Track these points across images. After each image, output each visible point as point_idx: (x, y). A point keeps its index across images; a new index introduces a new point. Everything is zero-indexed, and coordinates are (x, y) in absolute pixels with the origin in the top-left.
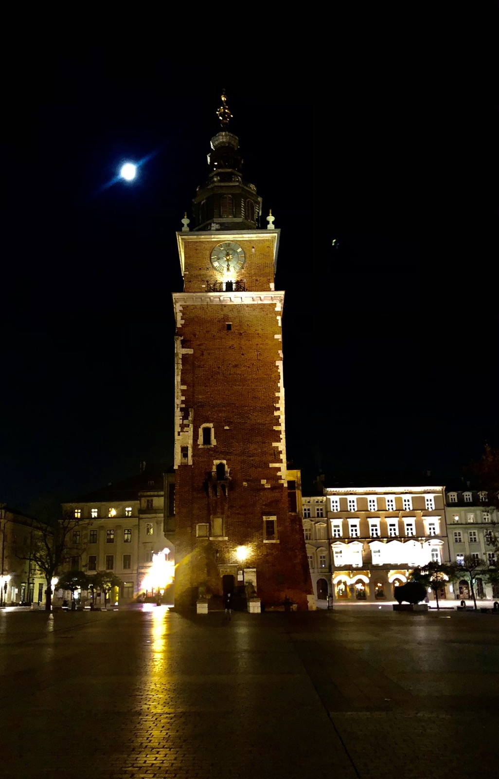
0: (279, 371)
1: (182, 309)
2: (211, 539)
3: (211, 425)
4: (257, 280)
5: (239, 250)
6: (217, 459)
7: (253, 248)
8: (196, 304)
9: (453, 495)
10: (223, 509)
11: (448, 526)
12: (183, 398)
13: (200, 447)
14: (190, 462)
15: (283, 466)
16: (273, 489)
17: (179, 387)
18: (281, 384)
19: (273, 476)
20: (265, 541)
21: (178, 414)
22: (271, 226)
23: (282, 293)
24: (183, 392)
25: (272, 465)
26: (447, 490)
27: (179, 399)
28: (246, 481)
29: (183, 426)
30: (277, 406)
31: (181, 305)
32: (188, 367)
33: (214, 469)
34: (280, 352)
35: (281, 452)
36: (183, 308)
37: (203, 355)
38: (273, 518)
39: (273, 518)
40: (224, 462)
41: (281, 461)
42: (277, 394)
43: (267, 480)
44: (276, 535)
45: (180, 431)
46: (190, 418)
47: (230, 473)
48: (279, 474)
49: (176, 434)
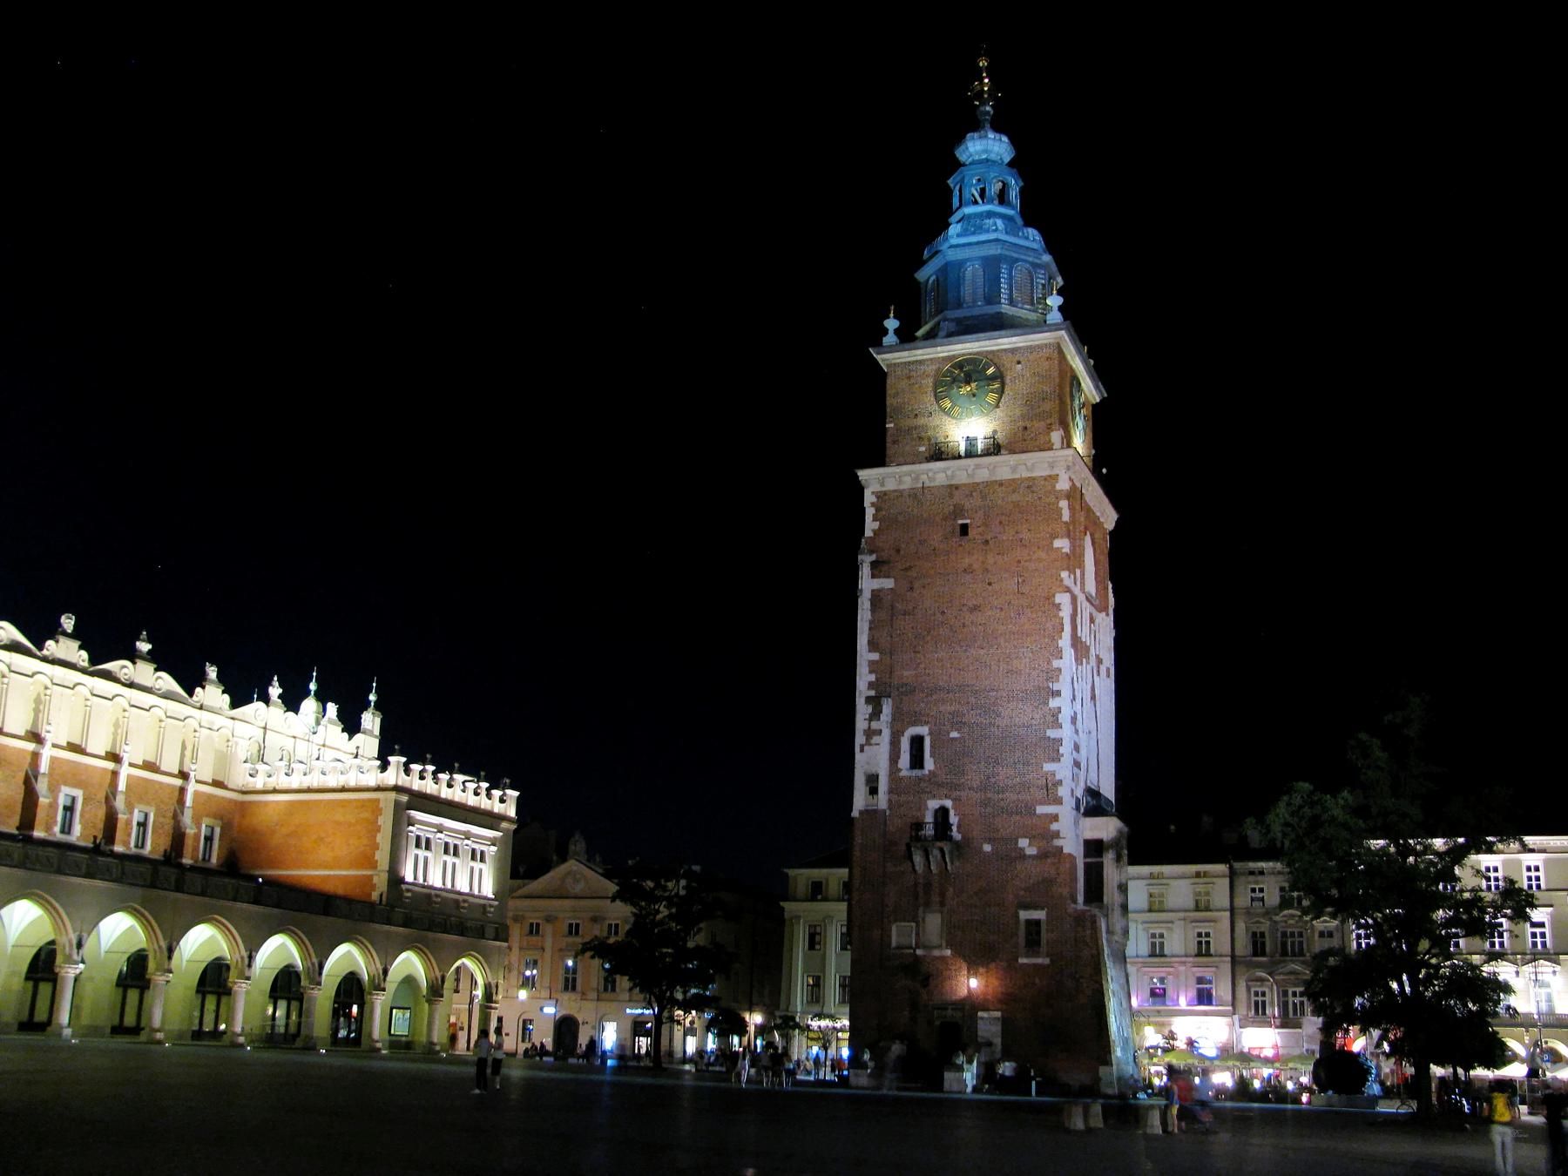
0: (1061, 614)
1: (874, 499)
2: (919, 952)
3: (923, 730)
5: (991, 371)
6: (934, 797)
10: (942, 895)
12: (872, 678)
13: (904, 773)
14: (882, 800)
16: (1043, 856)
17: (865, 656)
19: (1045, 834)
21: (862, 710)
25: (1040, 810)
27: (864, 679)
28: (990, 840)
29: (870, 733)
32: (883, 615)
33: (929, 818)
35: (1060, 782)
38: (1040, 915)
39: (1040, 915)
40: (948, 803)
42: (1056, 663)
43: (1032, 838)
44: (1044, 948)
47: (959, 827)
48: (1054, 827)
49: (857, 749)
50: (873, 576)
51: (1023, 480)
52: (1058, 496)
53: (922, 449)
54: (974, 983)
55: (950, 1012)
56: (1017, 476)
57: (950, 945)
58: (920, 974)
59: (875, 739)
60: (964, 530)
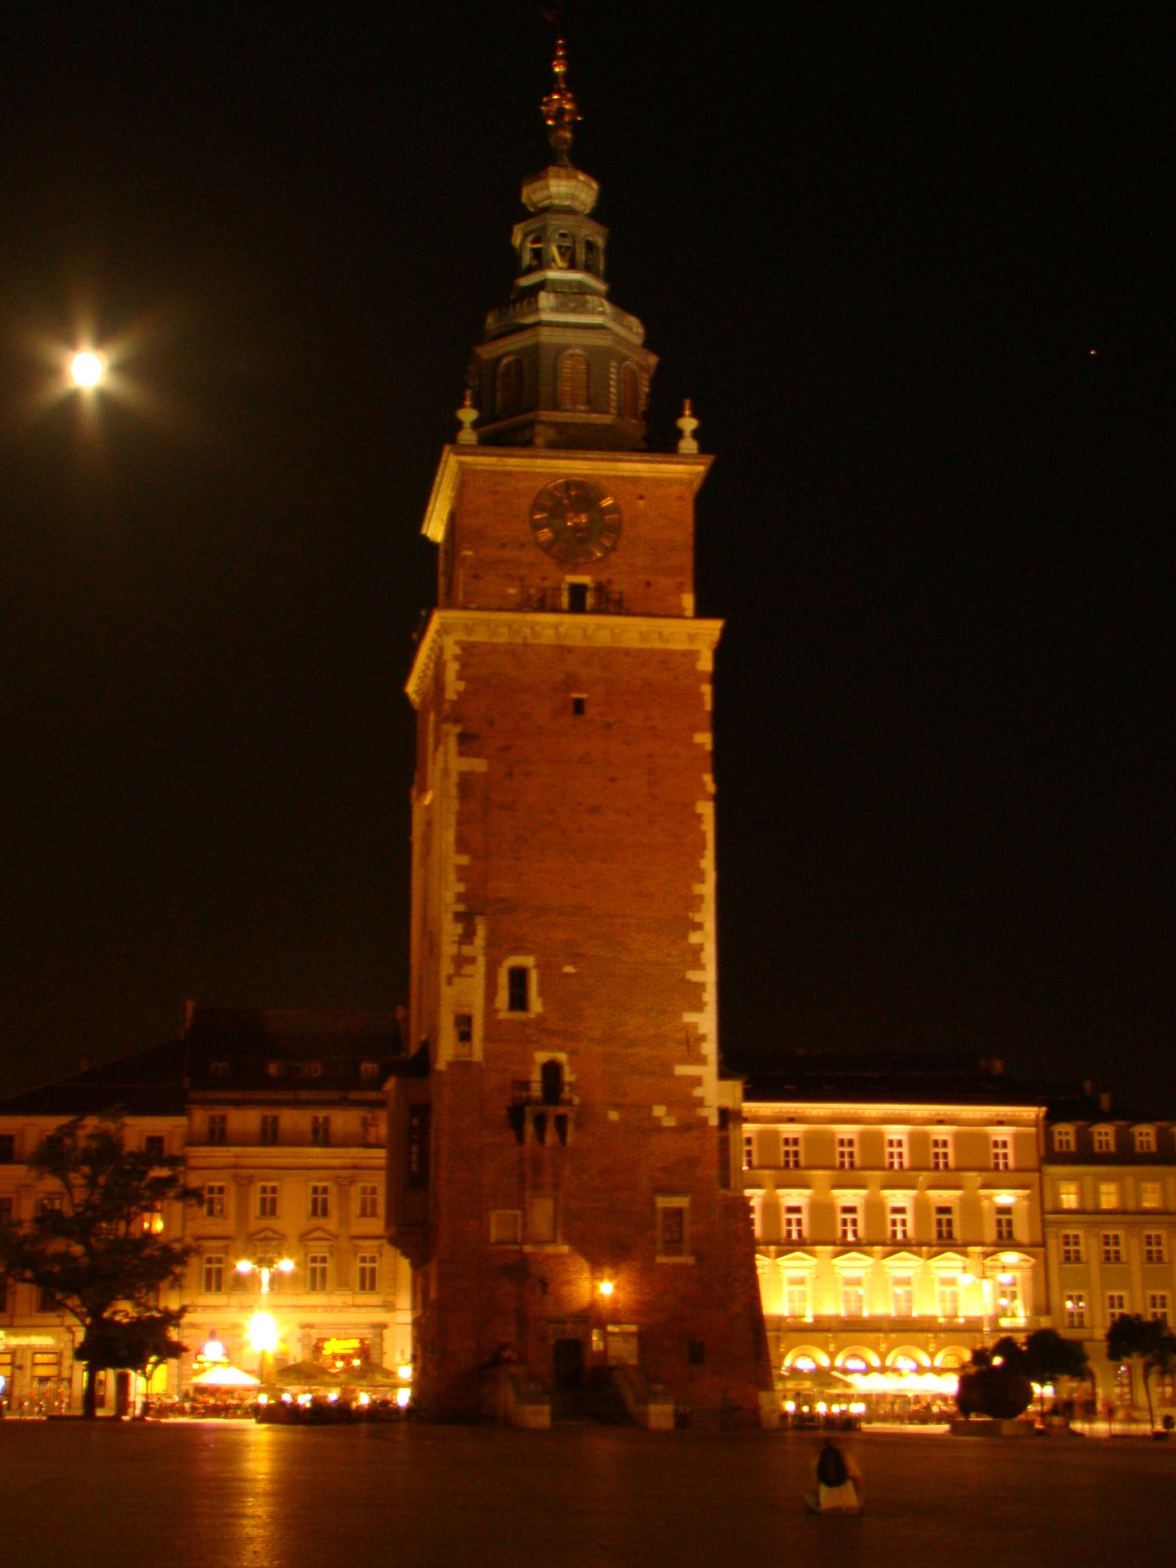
2: (528, 1248)
3: (528, 961)
4: (648, 584)
6: (543, 1048)
7: (641, 497)
8: (495, 640)
9: (1065, 1132)
11: (1050, 1217)
12: (461, 888)
14: (477, 1050)
15: (709, 1071)
18: (708, 863)
20: (661, 1259)
22: (688, 445)
23: (713, 628)
24: (463, 873)
25: (681, 1070)
26: (1051, 1118)
28: (616, 1106)
30: (698, 918)
31: (457, 643)
33: (536, 1076)
34: (708, 778)
35: (703, 1038)
36: (463, 649)
37: (510, 775)
38: (682, 1202)
39: (682, 1202)
40: (562, 1057)
41: (701, 1060)
43: (670, 1105)
45: (452, 971)
46: (480, 939)
48: (698, 1092)
50: (462, 754)
51: (654, 652)
52: (699, 677)
53: (512, 591)
54: (606, 1288)
55: (569, 1326)
56: (647, 646)
57: (569, 1240)
58: (529, 1277)
59: (468, 969)
60: (579, 706)
